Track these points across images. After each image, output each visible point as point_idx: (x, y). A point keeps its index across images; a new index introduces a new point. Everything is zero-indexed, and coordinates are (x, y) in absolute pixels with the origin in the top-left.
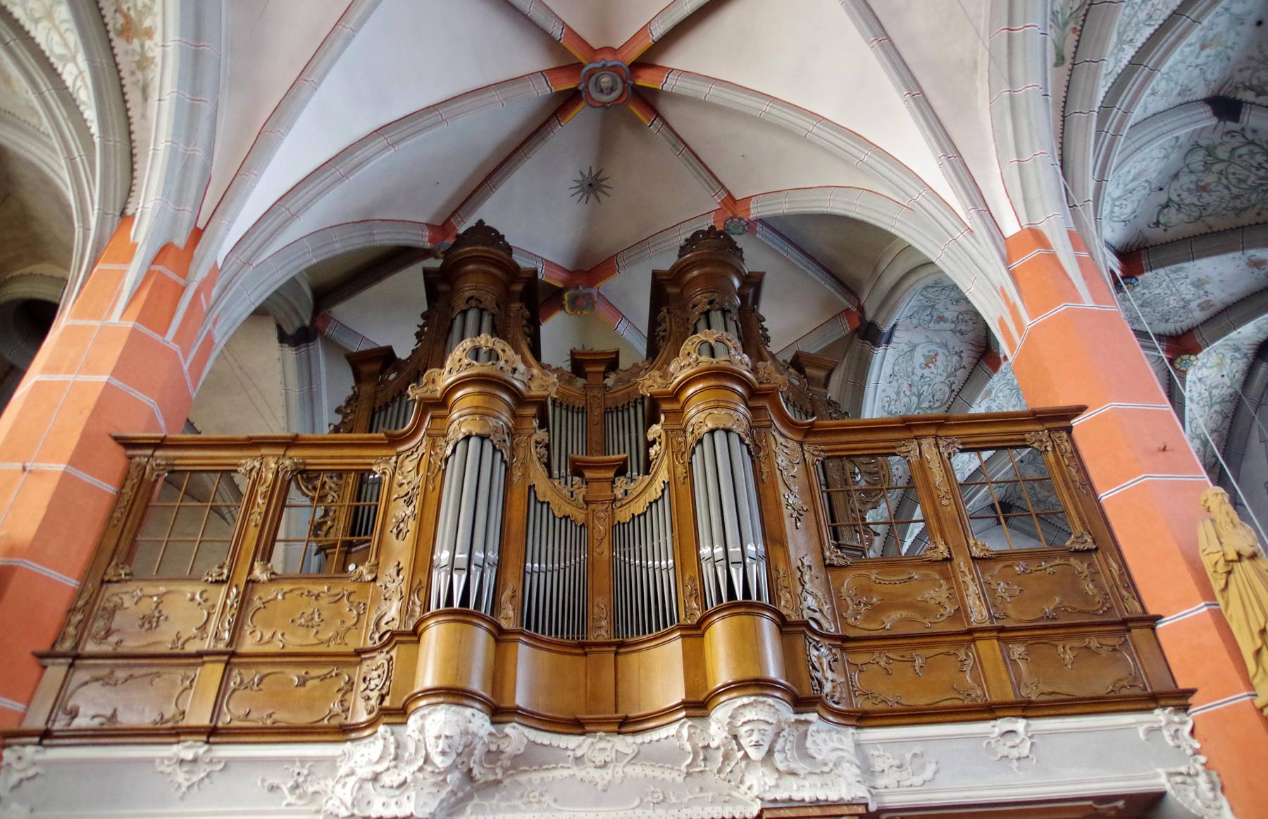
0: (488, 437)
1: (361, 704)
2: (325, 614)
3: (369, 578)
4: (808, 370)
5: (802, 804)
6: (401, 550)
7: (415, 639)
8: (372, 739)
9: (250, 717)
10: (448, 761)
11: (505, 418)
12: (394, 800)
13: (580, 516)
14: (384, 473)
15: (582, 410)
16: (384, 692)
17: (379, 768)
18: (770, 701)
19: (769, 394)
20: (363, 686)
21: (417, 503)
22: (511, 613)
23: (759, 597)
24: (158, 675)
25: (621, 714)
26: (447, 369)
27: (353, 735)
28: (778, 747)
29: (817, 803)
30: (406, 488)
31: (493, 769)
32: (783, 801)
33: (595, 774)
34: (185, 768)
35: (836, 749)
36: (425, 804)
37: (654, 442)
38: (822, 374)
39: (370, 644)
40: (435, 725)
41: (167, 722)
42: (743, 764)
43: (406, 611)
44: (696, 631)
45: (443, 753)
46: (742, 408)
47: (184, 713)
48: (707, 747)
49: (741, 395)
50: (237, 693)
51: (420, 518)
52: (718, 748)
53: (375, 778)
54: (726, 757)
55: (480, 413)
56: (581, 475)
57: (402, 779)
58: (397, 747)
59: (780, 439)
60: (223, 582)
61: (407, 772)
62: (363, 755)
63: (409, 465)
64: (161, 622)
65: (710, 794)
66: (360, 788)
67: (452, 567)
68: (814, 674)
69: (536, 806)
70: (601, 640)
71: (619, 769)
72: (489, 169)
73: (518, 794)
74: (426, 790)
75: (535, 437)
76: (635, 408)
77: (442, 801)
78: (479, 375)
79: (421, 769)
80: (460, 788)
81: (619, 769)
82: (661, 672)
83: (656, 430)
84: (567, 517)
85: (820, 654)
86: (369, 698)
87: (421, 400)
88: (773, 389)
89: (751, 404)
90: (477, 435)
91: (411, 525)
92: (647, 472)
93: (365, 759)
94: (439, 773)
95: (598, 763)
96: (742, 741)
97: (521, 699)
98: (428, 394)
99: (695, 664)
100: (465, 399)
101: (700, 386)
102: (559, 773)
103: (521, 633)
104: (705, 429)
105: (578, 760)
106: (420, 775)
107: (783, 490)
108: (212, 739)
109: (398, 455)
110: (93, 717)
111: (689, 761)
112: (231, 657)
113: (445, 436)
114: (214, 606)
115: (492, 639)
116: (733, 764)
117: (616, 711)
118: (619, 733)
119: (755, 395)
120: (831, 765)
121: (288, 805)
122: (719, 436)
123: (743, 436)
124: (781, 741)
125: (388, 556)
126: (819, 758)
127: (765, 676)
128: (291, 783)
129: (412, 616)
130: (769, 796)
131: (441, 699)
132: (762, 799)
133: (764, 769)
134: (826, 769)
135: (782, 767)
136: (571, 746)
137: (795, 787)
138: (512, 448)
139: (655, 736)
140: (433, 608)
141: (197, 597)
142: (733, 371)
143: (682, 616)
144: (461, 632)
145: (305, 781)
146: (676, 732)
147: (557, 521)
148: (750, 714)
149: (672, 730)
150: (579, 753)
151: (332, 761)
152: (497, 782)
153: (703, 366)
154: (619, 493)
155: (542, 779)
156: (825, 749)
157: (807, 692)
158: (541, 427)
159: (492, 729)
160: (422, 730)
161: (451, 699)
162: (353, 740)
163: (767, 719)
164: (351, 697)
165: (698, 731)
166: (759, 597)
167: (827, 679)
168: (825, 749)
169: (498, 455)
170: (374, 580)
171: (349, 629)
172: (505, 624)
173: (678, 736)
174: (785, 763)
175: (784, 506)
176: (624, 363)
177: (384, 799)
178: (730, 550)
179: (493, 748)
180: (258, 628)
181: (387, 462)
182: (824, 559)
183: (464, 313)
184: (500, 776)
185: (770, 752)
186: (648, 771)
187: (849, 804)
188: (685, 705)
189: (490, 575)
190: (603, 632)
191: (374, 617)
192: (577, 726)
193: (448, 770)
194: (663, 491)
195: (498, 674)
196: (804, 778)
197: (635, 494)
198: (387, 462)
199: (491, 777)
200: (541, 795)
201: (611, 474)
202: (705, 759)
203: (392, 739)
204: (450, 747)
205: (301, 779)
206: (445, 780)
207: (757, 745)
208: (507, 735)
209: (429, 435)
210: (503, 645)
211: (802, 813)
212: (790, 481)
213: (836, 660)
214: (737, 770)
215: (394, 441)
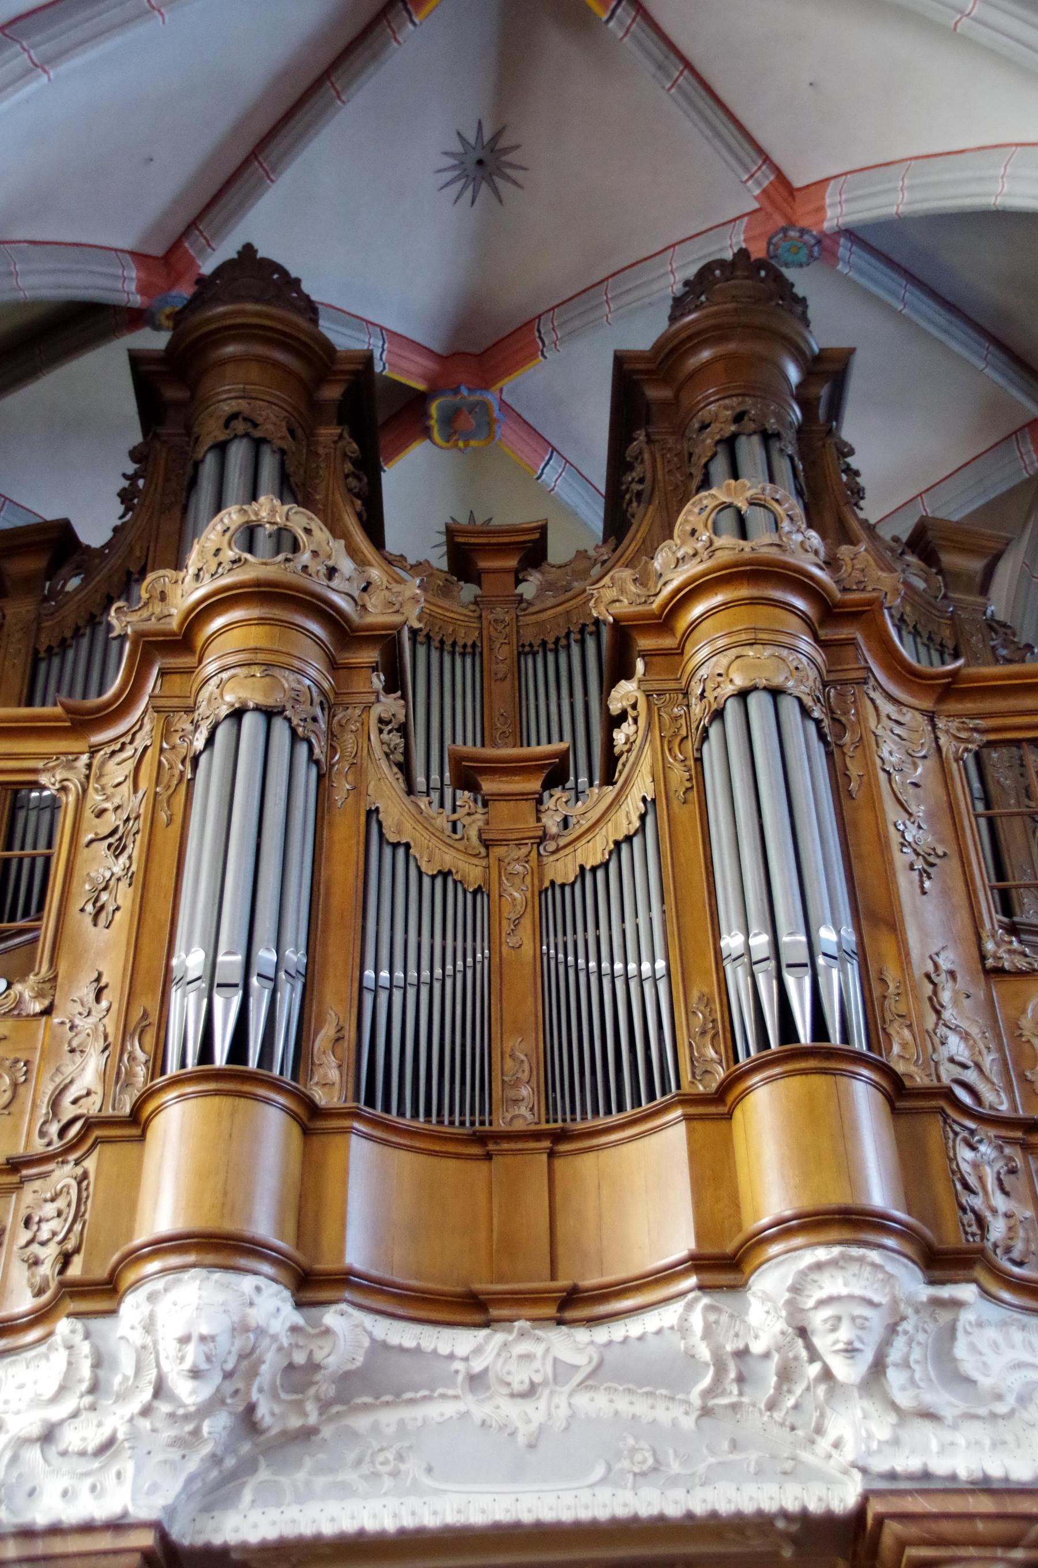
0: (281, 712)
1: (20, 1276)
3: (37, 1007)
4: (949, 559)
5: (952, 1487)
6: (103, 948)
7: (135, 1132)
8: (43, 1349)
10: (205, 1391)
11: (315, 669)
12: (88, 1482)
13: (472, 872)
14: (64, 789)
15: (473, 650)
16: (70, 1246)
17: (57, 1413)
18: (874, 1255)
19: (864, 614)
20: (25, 1236)
21: (135, 849)
22: (334, 1075)
23: (846, 1037)
26: (192, 570)
28: (895, 1354)
29: (984, 1487)
30: (111, 820)
31: (298, 1407)
32: (911, 1477)
33: (511, 1410)
35: (1019, 1365)
36: (154, 1488)
37: (623, 717)
38: (976, 565)
39: (38, 1146)
40: (178, 1314)
42: (821, 1390)
43: (116, 1076)
44: (714, 1108)
45: (195, 1374)
46: (805, 644)
48: (742, 1354)
49: (804, 617)
51: (143, 883)
52: (767, 1355)
53: (48, 1436)
54: (786, 1375)
55: (264, 662)
56: (473, 787)
57: (104, 1434)
58: (97, 1364)
59: (887, 708)
61: (116, 1418)
63: (117, 771)
65: (753, 1456)
66: (15, 1459)
67: (212, 983)
68: (966, 1199)
69: (388, 1483)
70: (519, 1126)
71: (561, 1400)
72: (261, 126)
73: (351, 1456)
74: (157, 1457)
75: (377, 711)
76: (582, 643)
77: (191, 1480)
78: (258, 583)
79: (146, 1411)
80: (230, 1448)
81: (561, 1400)
82: (643, 1191)
83: (625, 692)
84: (445, 875)
85: (979, 1158)
86: (36, 1263)
87: (139, 635)
88: (870, 602)
89: (824, 634)
90: (257, 709)
91: (124, 896)
92: (608, 780)
93: (28, 1394)
94: (187, 1417)
95: (517, 1387)
96: (818, 1341)
97: (356, 1254)
98: (153, 625)
99: (714, 1176)
100: (230, 634)
101: (718, 599)
102: (437, 1411)
103: (356, 1115)
104: (729, 689)
105: (476, 1381)
106: (145, 1424)
107: (892, 813)
109: (93, 751)
111: (706, 1381)
113: (190, 710)
115: (296, 1131)
116: (799, 1390)
117: (553, 1277)
118: (560, 1322)
119: (833, 615)
122: (758, 703)
123: (808, 701)
124: (899, 1344)
125: (76, 963)
126: (985, 1382)
127: (862, 1202)
129: (128, 1085)
130: (879, 1465)
131: (191, 1258)
132: (864, 1471)
133: (866, 1404)
134: (1001, 1408)
135: (904, 1400)
136: (461, 1351)
137: (934, 1445)
138: (332, 736)
139: (634, 1327)
140: (172, 1068)
142: (786, 566)
143: (686, 1076)
144: (233, 1114)
147: (426, 881)
148: (833, 1284)
149: (669, 1316)
152: (307, 1434)
153: (723, 557)
154: (551, 823)
155: (402, 1424)
156: (998, 1363)
157: (952, 1238)
158: (389, 689)
159: (297, 1318)
160: (149, 1326)
161: (210, 1258)
163: (869, 1294)
165: (724, 1318)
166: (846, 1037)
167: (994, 1211)
168: (998, 1363)
169: (303, 749)
170: (48, 1011)
172: (321, 1098)
173: (683, 1329)
174: (912, 1392)
175: (895, 847)
176: (558, 551)
177: (65, 1482)
178: (784, 939)
179: (299, 1358)
181: (69, 766)
182: (983, 958)
183: (221, 448)
184: (313, 1419)
185: (878, 1367)
186: (622, 1404)
188: (698, 1263)
189: (289, 997)
190: (523, 1110)
191: (48, 1089)
192: (472, 1308)
193: (206, 1410)
194: (643, 818)
195: (310, 1200)
196: (955, 1427)
197: (585, 824)
198: (69, 766)
199: (295, 1422)
201: (535, 785)
202: (741, 1379)
203: (85, 1348)
204: (208, 1359)
206: (196, 1432)
207: (850, 1351)
208: (327, 1332)
209: (157, 710)
210: (316, 1141)
212: (908, 795)
213: (1012, 1171)
214: (809, 1405)
215: (83, 722)
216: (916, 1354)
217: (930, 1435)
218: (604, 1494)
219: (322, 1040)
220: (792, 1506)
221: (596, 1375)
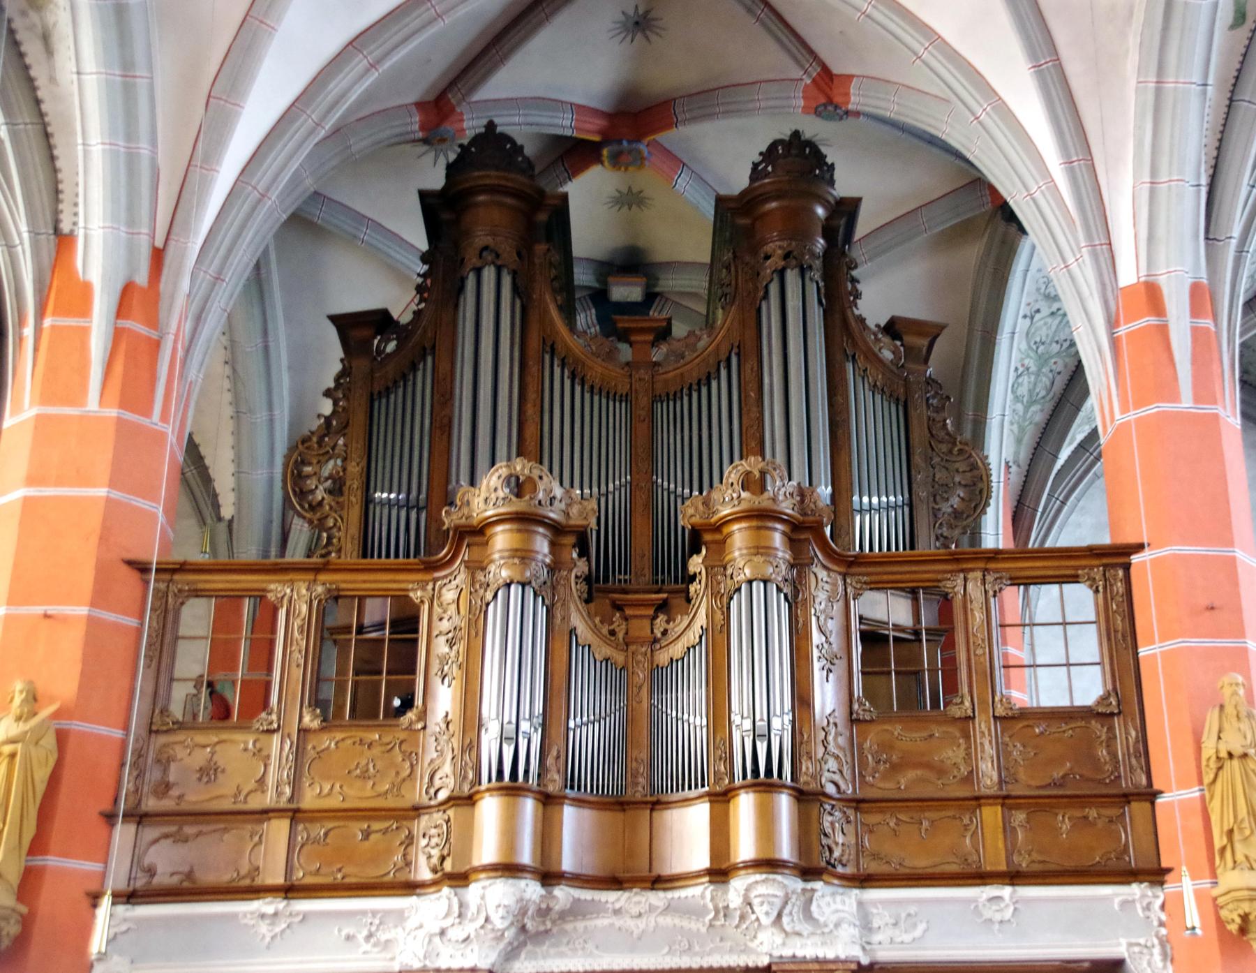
1: (422, 859)
2: (379, 765)
3: (420, 726)
5: (804, 960)
9: (322, 871)
20: (424, 842)
24: (226, 830)
25: (654, 873)
27: (418, 891)
28: (786, 911)
29: (817, 960)
31: (544, 923)
33: (630, 923)
34: (268, 921)
41: (243, 878)
42: (756, 924)
44: (721, 799)
47: (258, 869)
50: (305, 848)
54: (743, 918)
60: (274, 731)
62: (432, 908)
64: (219, 775)
68: (824, 841)
69: (580, 952)
73: (565, 941)
78: (517, 513)
80: (516, 937)
81: (652, 919)
105: (617, 912)
108: (289, 895)
110: (172, 874)
111: (712, 915)
112: (295, 815)
114: (268, 757)
116: (748, 922)
118: (653, 889)
120: (831, 926)
121: (364, 953)
126: (822, 920)
128: (365, 933)
130: (776, 953)
133: (774, 930)
135: (788, 928)
137: (799, 945)
141: (250, 746)
145: (377, 930)
146: (700, 892)
150: (617, 906)
151: (400, 916)
152: (547, 932)
155: (586, 927)
162: (418, 895)
164: (413, 849)
167: (837, 844)
170: (424, 728)
171: (404, 780)
173: (703, 896)
180: (316, 779)
185: (779, 916)
186: (677, 921)
187: (845, 962)
189: (536, 739)
192: (614, 882)
195: (547, 837)
196: (808, 937)
199: (542, 928)
200: (585, 942)
205: (373, 929)
206: (503, 935)
211: (804, 967)
214: (751, 928)
216: (796, 909)
217: (797, 941)
218: (668, 959)
219: (550, 761)
220: (742, 964)
221: (668, 909)
